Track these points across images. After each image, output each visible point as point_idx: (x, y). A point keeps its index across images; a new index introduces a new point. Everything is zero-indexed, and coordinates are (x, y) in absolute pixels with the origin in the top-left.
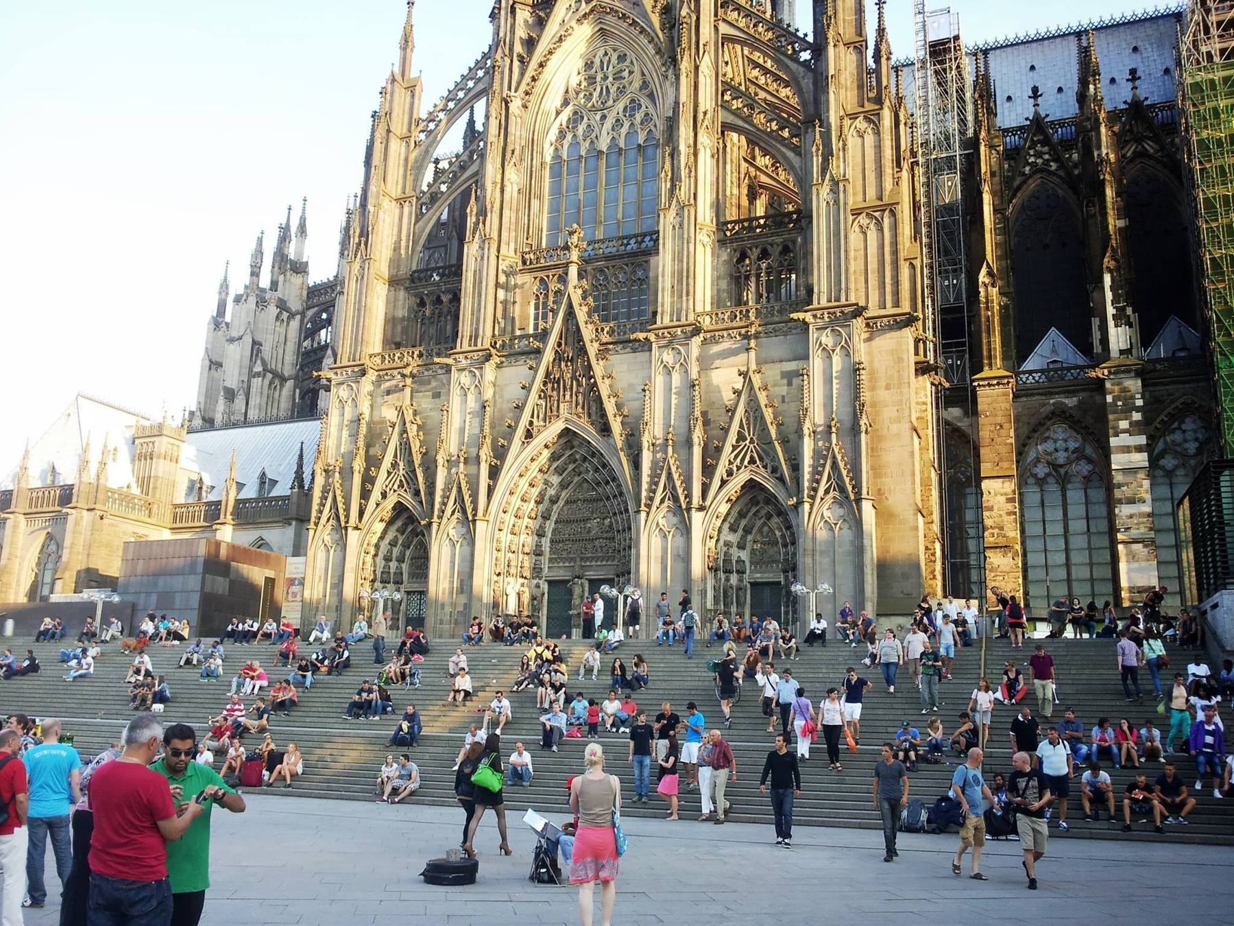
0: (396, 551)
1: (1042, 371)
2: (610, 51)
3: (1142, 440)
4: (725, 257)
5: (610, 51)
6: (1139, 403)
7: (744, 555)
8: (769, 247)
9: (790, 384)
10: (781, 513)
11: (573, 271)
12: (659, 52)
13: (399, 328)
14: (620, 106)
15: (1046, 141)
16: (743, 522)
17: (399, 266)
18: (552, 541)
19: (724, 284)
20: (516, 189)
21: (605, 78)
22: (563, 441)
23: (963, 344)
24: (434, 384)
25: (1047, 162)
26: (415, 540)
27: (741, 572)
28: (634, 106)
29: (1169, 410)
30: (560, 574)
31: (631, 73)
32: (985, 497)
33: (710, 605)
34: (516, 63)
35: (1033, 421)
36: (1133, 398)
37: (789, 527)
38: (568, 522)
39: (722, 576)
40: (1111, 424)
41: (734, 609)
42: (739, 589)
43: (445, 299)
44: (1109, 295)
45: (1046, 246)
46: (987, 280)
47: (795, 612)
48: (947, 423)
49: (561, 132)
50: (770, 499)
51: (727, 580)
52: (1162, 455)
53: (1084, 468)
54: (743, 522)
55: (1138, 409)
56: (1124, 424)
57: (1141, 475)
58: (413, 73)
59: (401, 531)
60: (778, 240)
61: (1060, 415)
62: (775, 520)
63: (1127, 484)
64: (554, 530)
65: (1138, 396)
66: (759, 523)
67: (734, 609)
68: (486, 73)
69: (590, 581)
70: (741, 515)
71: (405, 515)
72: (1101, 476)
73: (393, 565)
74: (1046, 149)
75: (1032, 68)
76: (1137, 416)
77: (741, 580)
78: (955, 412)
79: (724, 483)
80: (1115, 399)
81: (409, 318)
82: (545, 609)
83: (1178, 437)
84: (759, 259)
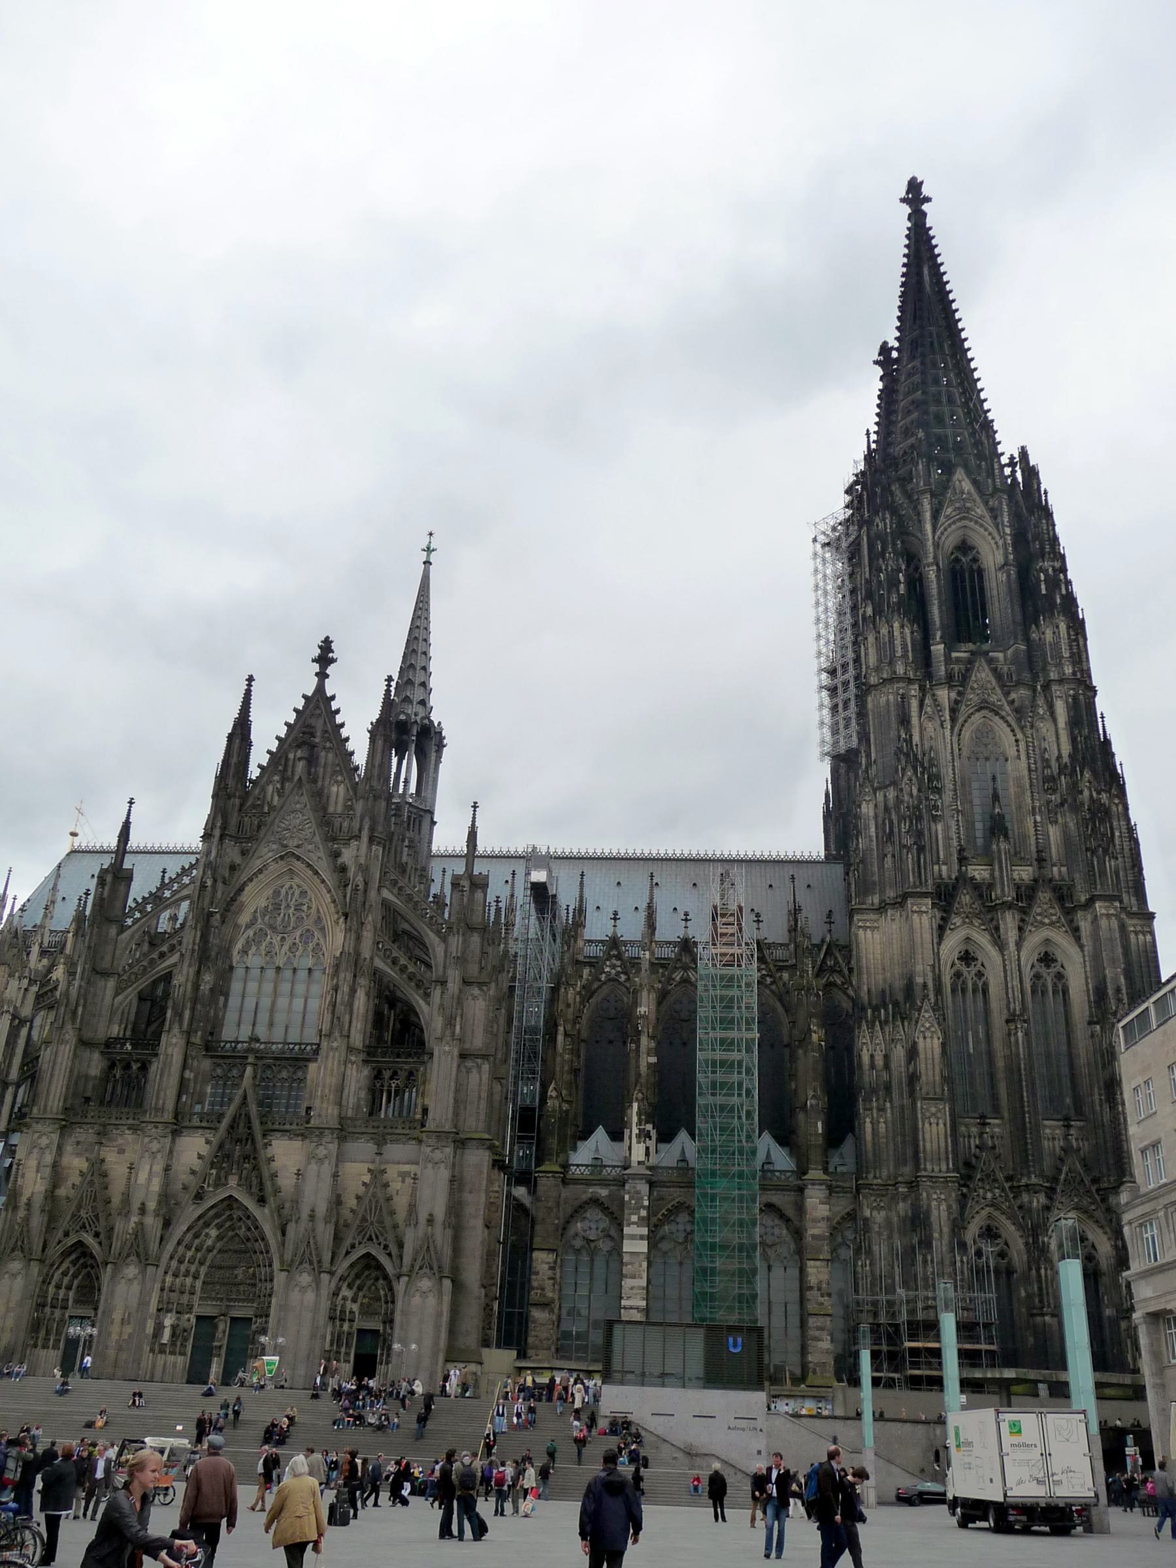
0: (66, 1280)
1: (587, 1166)
2: (295, 887)
4: (366, 1071)
5: (295, 887)
7: (355, 1307)
8: (399, 1072)
9: (403, 1181)
10: (386, 1277)
11: (249, 1070)
12: (334, 901)
13: (90, 1086)
14: (298, 933)
15: (619, 957)
16: (358, 1282)
17: (96, 1031)
18: (204, 1283)
19: (363, 1094)
20: (208, 987)
21: (288, 906)
22: (226, 1203)
23: (532, 1138)
24: (120, 1141)
25: (618, 974)
26: (84, 1272)
27: (351, 1321)
28: (307, 936)
29: (669, 1206)
30: (209, 1311)
31: (309, 908)
32: (534, 1264)
33: (327, 1347)
34: (220, 886)
35: (577, 1203)
36: (642, 1199)
37: (391, 1289)
38: (220, 1268)
39: (338, 1323)
41: (343, 1350)
42: (349, 1334)
43: (135, 1067)
45: (611, 1042)
46: (554, 1094)
47: (388, 1355)
48: (515, 1199)
49: (247, 942)
50: (379, 1267)
51: (341, 1326)
52: (663, 1238)
53: (605, 1246)
54: (358, 1282)
55: (644, 1207)
56: (634, 1218)
57: (642, 1257)
58: (127, 865)
59: (74, 1263)
60: (407, 1067)
61: (595, 1202)
62: (381, 1282)
63: (631, 1264)
64: (206, 1275)
66: (369, 1283)
67: (343, 1350)
68: (192, 882)
69: (233, 1319)
70: (357, 1276)
71: (79, 1250)
72: (617, 1250)
73: (62, 1292)
74: (618, 963)
75: (619, 883)
77: (351, 1327)
78: (520, 1192)
79: (348, 1253)
81: (101, 1079)
82: (191, 1341)
83: (673, 1227)
84: (391, 1078)
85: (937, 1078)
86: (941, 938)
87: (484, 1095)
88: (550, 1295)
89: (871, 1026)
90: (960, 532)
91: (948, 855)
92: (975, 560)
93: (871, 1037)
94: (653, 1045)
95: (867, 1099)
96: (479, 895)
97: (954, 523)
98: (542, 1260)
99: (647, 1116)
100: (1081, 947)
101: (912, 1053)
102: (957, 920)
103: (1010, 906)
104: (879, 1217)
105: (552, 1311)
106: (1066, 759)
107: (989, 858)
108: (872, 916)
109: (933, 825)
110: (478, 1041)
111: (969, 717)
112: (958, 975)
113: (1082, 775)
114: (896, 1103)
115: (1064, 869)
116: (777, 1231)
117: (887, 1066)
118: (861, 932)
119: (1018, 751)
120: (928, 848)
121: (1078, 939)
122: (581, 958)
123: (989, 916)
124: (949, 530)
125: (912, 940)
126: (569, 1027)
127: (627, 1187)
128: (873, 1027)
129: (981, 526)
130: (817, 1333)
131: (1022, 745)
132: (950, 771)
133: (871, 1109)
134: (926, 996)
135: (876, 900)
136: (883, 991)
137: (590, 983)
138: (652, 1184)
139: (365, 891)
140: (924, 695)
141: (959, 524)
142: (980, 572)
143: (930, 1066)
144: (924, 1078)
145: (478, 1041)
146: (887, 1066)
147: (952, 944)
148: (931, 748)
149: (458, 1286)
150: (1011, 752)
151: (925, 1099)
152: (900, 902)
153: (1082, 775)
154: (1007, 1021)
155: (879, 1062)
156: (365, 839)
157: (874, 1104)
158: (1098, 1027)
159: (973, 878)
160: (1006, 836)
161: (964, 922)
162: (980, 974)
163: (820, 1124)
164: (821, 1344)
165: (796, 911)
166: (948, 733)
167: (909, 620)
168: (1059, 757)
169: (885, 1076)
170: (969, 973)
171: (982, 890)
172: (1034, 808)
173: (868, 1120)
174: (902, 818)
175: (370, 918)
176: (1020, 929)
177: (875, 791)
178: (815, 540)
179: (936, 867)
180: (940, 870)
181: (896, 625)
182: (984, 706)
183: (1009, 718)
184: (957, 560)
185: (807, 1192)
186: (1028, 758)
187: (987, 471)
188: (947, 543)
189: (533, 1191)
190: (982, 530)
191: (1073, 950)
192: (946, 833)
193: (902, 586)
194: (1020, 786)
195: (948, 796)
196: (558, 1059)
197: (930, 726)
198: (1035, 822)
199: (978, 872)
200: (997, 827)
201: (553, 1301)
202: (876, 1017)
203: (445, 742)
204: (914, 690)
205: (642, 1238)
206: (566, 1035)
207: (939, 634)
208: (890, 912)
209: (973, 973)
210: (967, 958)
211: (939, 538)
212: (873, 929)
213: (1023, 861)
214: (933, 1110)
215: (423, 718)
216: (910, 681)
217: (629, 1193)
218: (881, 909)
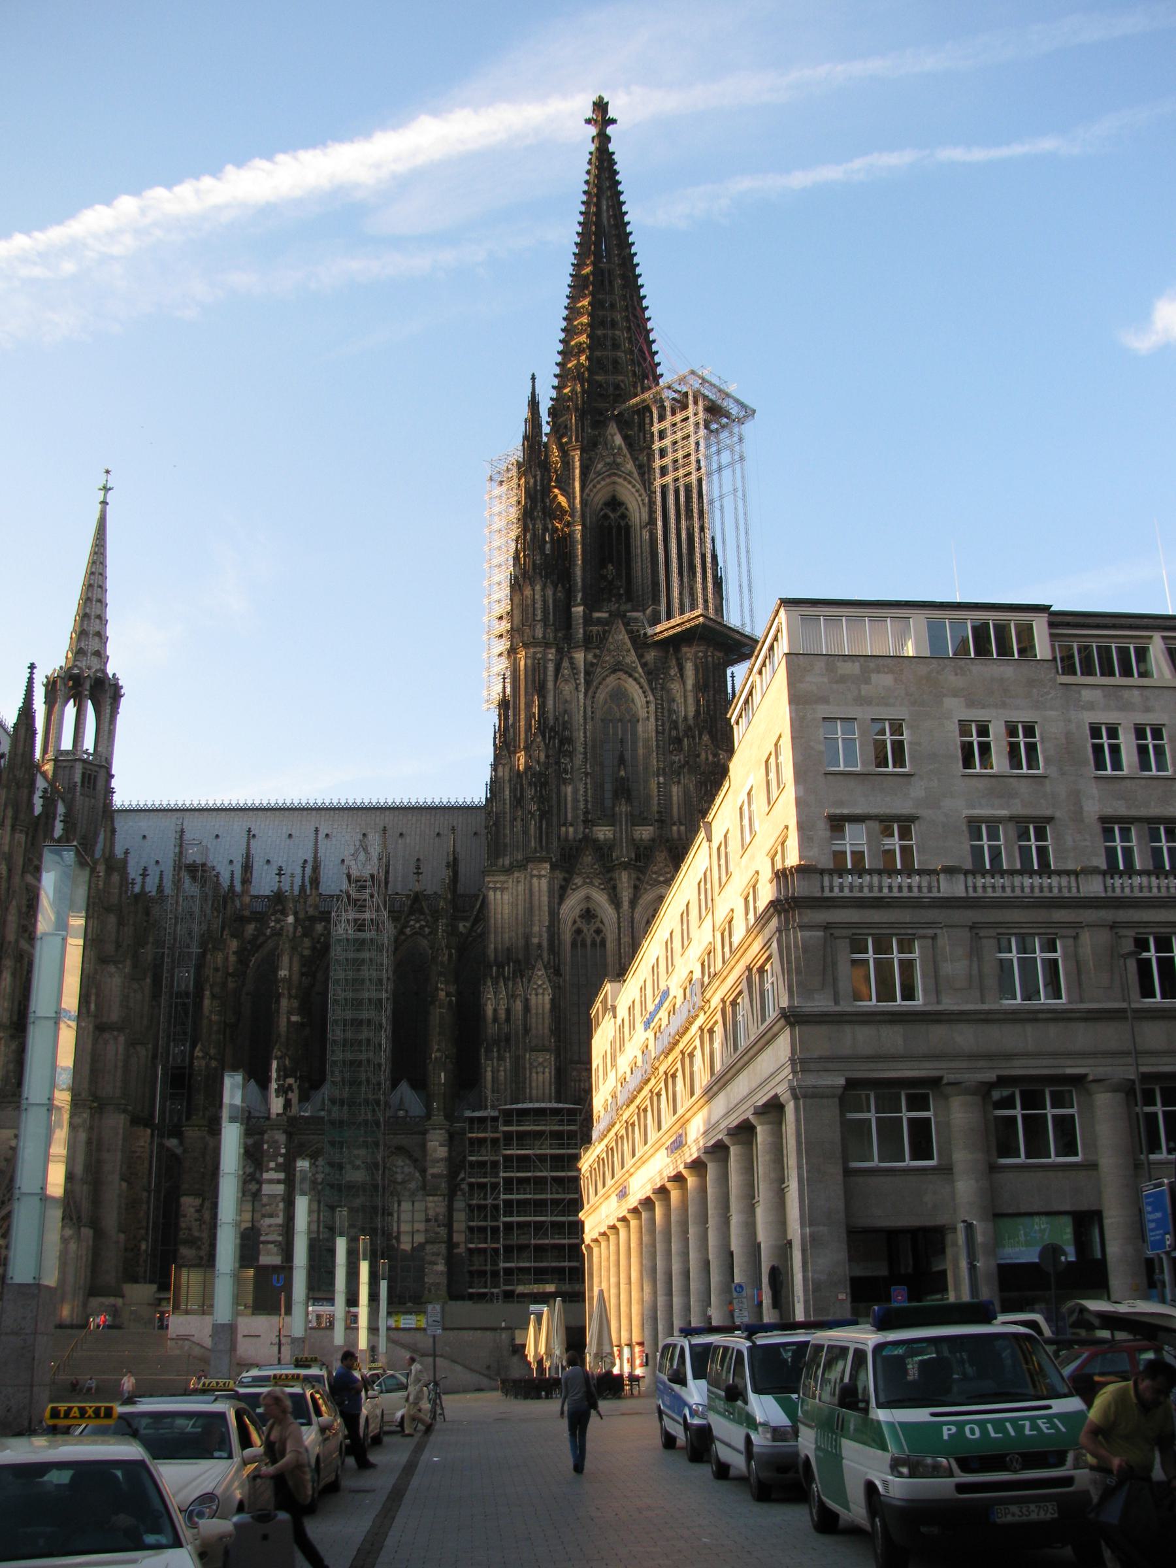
3: (282, 1176)
6: (283, 1151)
36: (279, 1147)
44: (274, 1075)
46: (200, 1054)
48: (168, 1149)
56: (272, 1165)
57: (279, 1198)
63: (270, 1205)
75: (290, 835)
76: (281, 1160)
78: (172, 1143)
80: (269, 1147)
85: (546, 1031)
86: (562, 899)
87: (120, 1064)
88: (196, 1234)
89: (496, 983)
90: (610, 488)
91: (575, 817)
92: (624, 516)
93: (495, 993)
94: (295, 1003)
95: (489, 1050)
96: (116, 878)
97: (603, 479)
98: (189, 1203)
99: (284, 1073)
101: (527, 1008)
102: (578, 881)
103: (625, 866)
105: (199, 1248)
106: (691, 722)
107: (612, 820)
108: (502, 878)
109: (563, 787)
110: (114, 1015)
111: (604, 679)
112: (579, 932)
113: (700, 738)
115: (682, 828)
116: (406, 1170)
117: (508, 1020)
118: (491, 893)
120: (555, 811)
122: (247, 913)
123: (608, 876)
124: (599, 486)
125: (531, 903)
126: (217, 990)
127: (266, 1137)
128: (497, 983)
129: (630, 482)
130: (433, 1259)
131: (652, 707)
132: (582, 734)
133: (492, 1060)
134: (540, 956)
135: (507, 862)
136: (508, 949)
137: (255, 937)
138: (290, 1135)
139: (9, 877)
140: (561, 659)
141: (608, 480)
142: (628, 528)
143: (540, 1021)
144: (534, 1032)
145: (114, 1015)
146: (508, 1020)
147: (571, 907)
148: (565, 711)
149: (99, 1234)
150: (642, 713)
151: (532, 1050)
152: (522, 866)
153: (700, 738)
155: (502, 1015)
156: (9, 828)
157: (495, 1054)
159: (596, 841)
160: (629, 800)
161: (585, 883)
162: (598, 931)
163: (443, 1075)
164: (435, 1267)
165: (454, 865)
166: (581, 696)
167: (552, 583)
168: (686, 718)
169: (506, 1028)
170: (588, 931)
171: (603, 851)
172: (658, 769)
173: (489, 1069)
174: (530, 784)
175: (14, 903)
176: (636, 887)
178: (491, 479)
179: (563, 829)
180: (567, 832)
181: (538, 588)
182: (618, 667)
183: (642, 680)
184: (606, 517)
185: (429, 1136)
186: (657, 720)
187: (639, 426)
188: (596, 499)
189: (181, 1143)
190: (630, 487)
192: (574, 794)
193: (548, 546)
194: (647, 747)
195: (578, 759)
196: (205, 1022)
197: (567, 689)
198: (659, 783)
199: (603, 833)
200: (624, 790)
201: (200, 1239)
202: (500, 974)
203: (123, 691)
204: (551, 654)
205: (279, 1182)
206: (213, 996)
207: (580, 595)
209: (592, 931)
210: (588, 915)
211: (588, 495)
212: (502, 890)
213: (644, 822)
214: (541, 1060)
215: (97, 671)
216: (547, 645)
218: (508, 871)
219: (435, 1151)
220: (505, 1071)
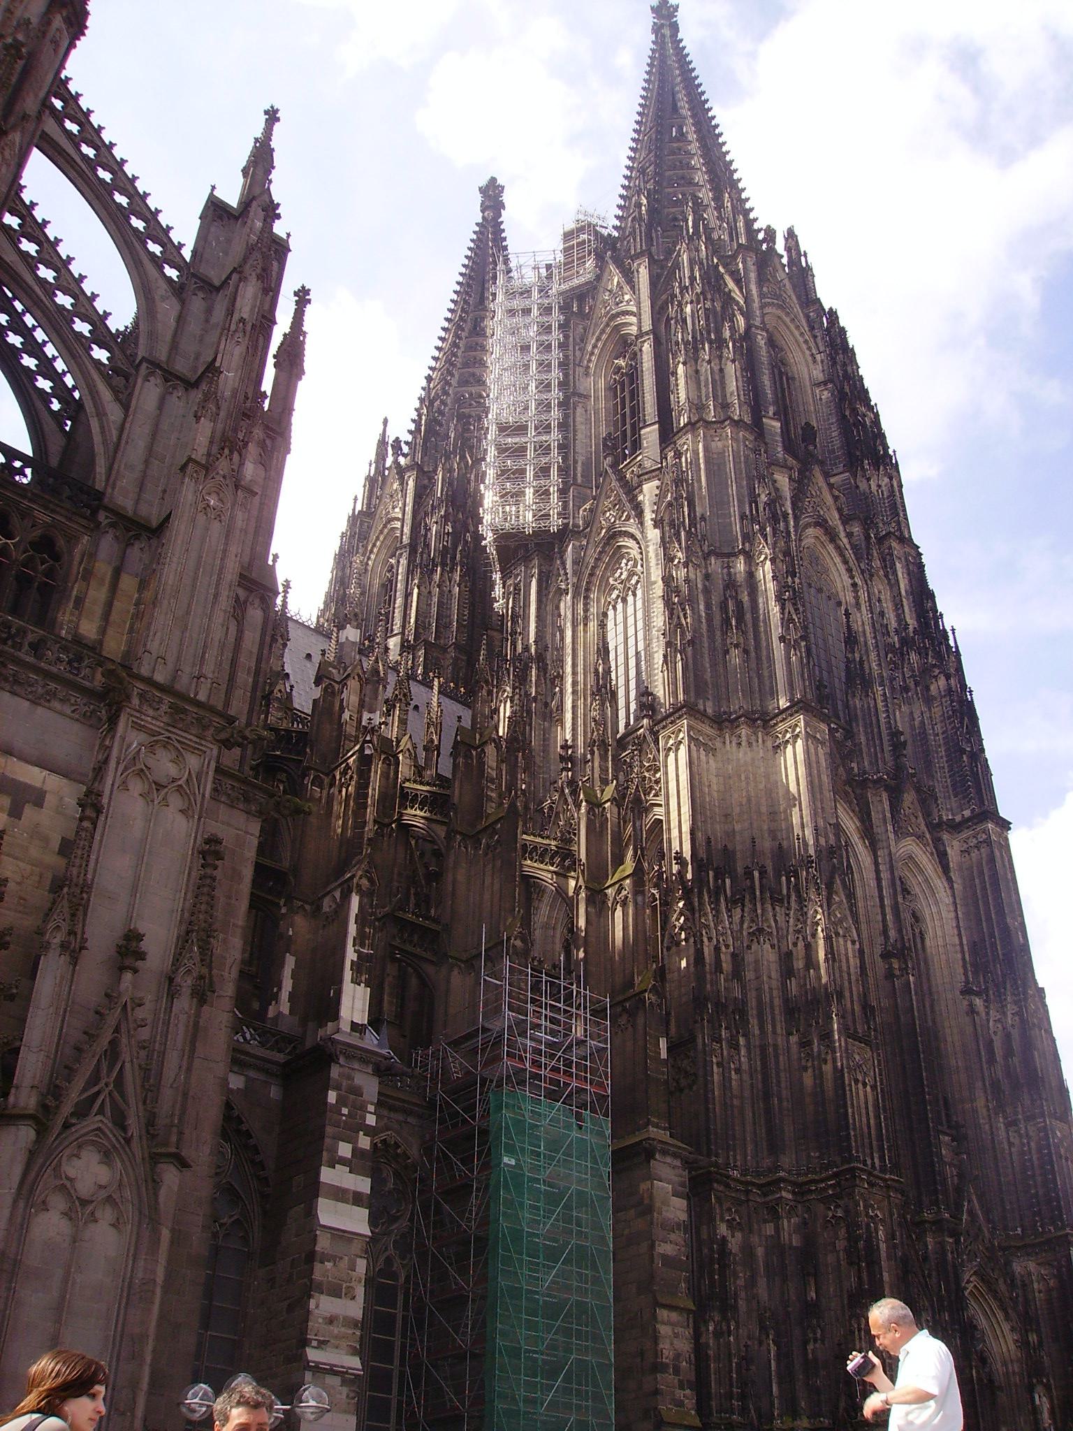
8: (15, 520)
36: (363, 1109)
40: (327, 1141)
55: (369, 1131)
56: (345, 1150)
60: (43, 517)
65: (371, 1108)
80: (341, 1101)
100: (950, 880)
104: (735, 1242)
114: (756, 1042)
119: (857, 598)
121: (946, 869)
128: (717, 902)
146: (737, 973)
154: (886, 956)
158: (978, 1002)
163: (663, 1043)
177: (706, 557)
182: (821, 523)
190: (797, 333)
191: (939, 884)
207: (771, 410)
208: (744, 731)
217: (337, 1088)
219: (666, 1203)
220: (738, 1071)
